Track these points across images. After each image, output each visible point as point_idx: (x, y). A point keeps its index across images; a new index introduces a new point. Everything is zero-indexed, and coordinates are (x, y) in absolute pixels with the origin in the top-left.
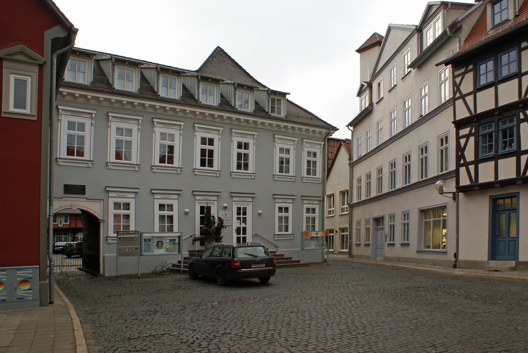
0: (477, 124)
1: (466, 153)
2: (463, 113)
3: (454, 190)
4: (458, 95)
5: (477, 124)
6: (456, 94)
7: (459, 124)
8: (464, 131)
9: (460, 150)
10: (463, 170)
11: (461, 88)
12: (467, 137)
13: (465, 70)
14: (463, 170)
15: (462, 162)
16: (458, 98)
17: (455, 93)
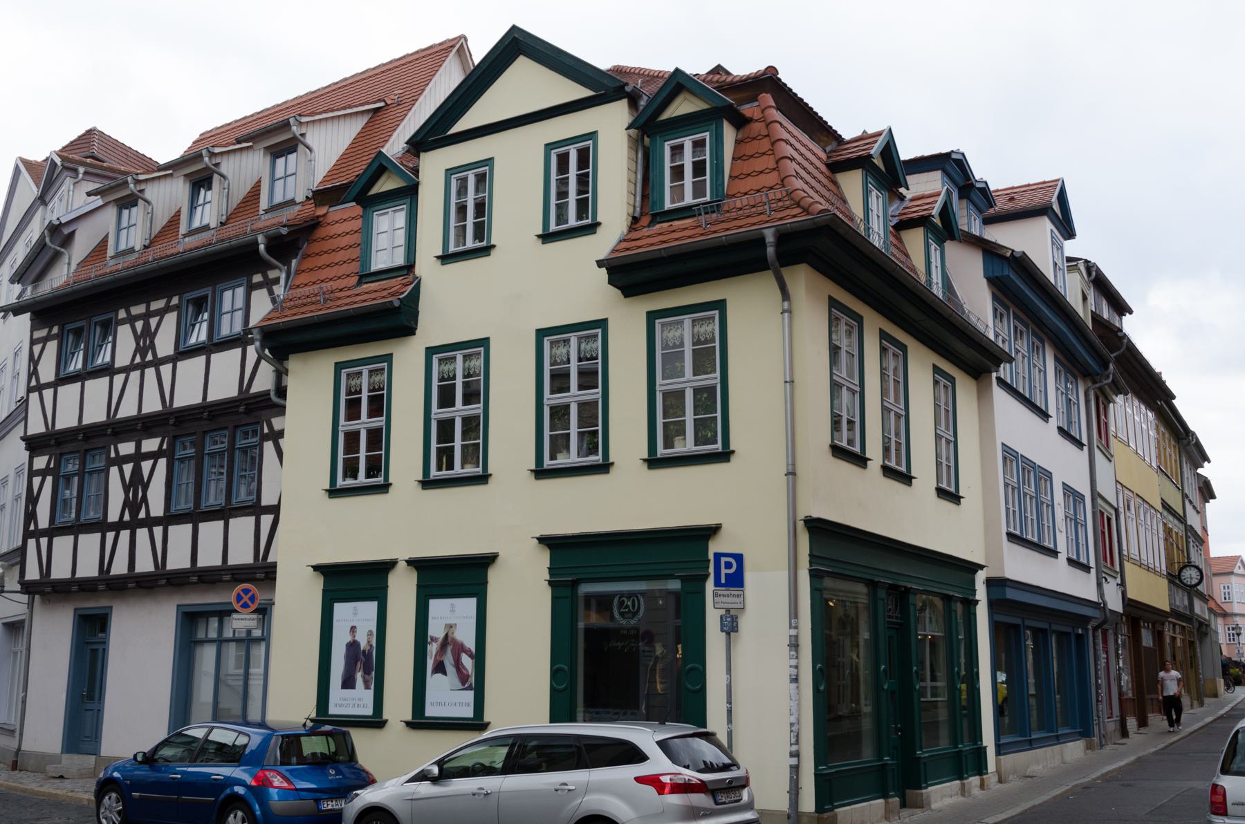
4: (33, 383)
7: (34, 445)
8: (41, 462)
10: (32, 543)
12: (43, 473)
15: (32, 528)
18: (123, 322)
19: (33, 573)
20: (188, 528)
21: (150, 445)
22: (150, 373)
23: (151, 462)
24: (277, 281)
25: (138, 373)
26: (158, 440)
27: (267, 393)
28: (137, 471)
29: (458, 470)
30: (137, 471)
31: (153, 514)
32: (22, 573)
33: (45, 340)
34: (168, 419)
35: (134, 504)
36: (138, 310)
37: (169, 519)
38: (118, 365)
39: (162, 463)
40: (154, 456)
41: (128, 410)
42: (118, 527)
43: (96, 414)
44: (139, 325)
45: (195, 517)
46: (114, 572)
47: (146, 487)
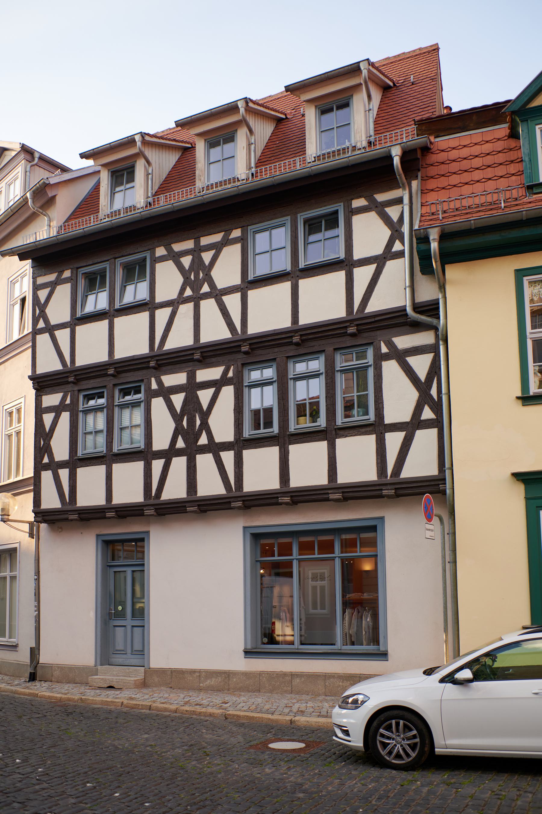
0: (76, 388)
1: (53, 443)
2: (49, 363)
3: (31, 517)
4: (41, 324)
5: (76, 388)
6: (38, 321)
7: (42, 383)
8: (52, 400)
9: (43, 437)
10: (47, 476)
11: (48, 311)
12: (57, 410)
13: (57, 278)
14: (47, 476)
15: (46, 460)
16: (41, 331)
17: (35, 321)
18: (163, 259)
20: (273, 452)
21: (214, 373)
25: (190, 306)
27: (403, 309)
28: (192, 402)
30: (192, 402)
31: (218, 439)
33: (53, 285)
34: (240, 346)
36: (189, 244)
37: (240, 444)
38: (159, 298)
40: (217, 385)
44: (186, 261)
46: (166, 496)
47: (206, 415)
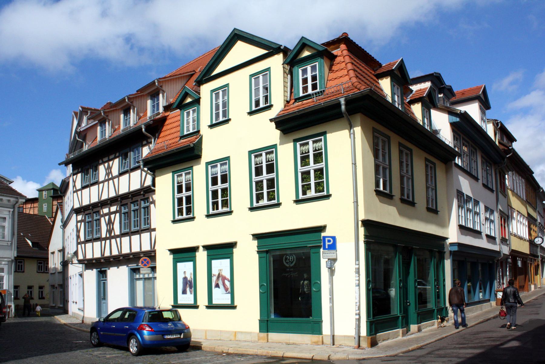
12: (81, 221)
18: (101, 164)
19: (81, 257)
21: (113, 209)
22: (111, 182)
23: (114, 215)
24: (151, 143)
25: (107, 182)
26: (116, 207)
28: (110, 219)
29: (221, 210)
30: (110, 219)
32: (77, 257)
33: (76, 174)
35: (110, 231)
36: (105, 159)
37: (122, 235)
39: (118, 215)
40: (115, 213)
41: (104, 197)
42: (106, 239)
43: (95, 200)
45: (129, 234)
